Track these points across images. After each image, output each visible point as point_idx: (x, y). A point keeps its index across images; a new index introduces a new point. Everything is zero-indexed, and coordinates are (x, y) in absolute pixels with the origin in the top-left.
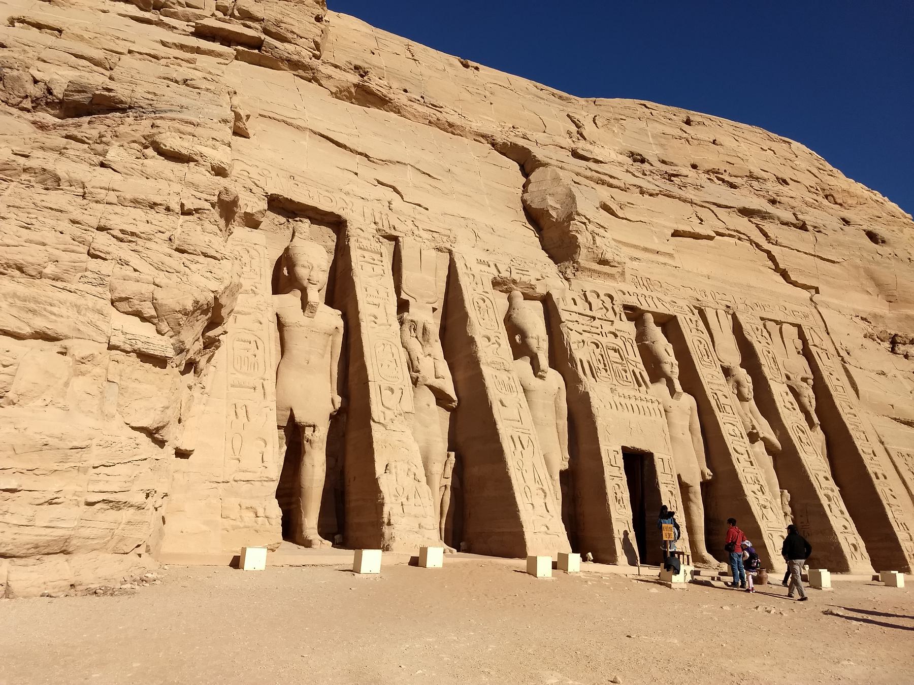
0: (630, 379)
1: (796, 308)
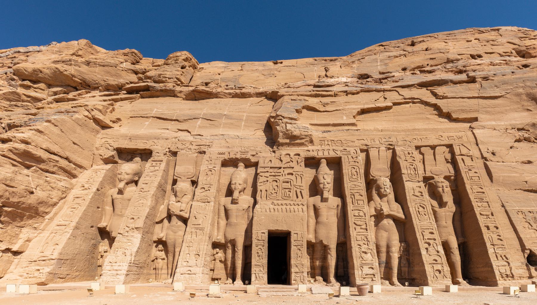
0: (291, 195)
1: (451, 134)
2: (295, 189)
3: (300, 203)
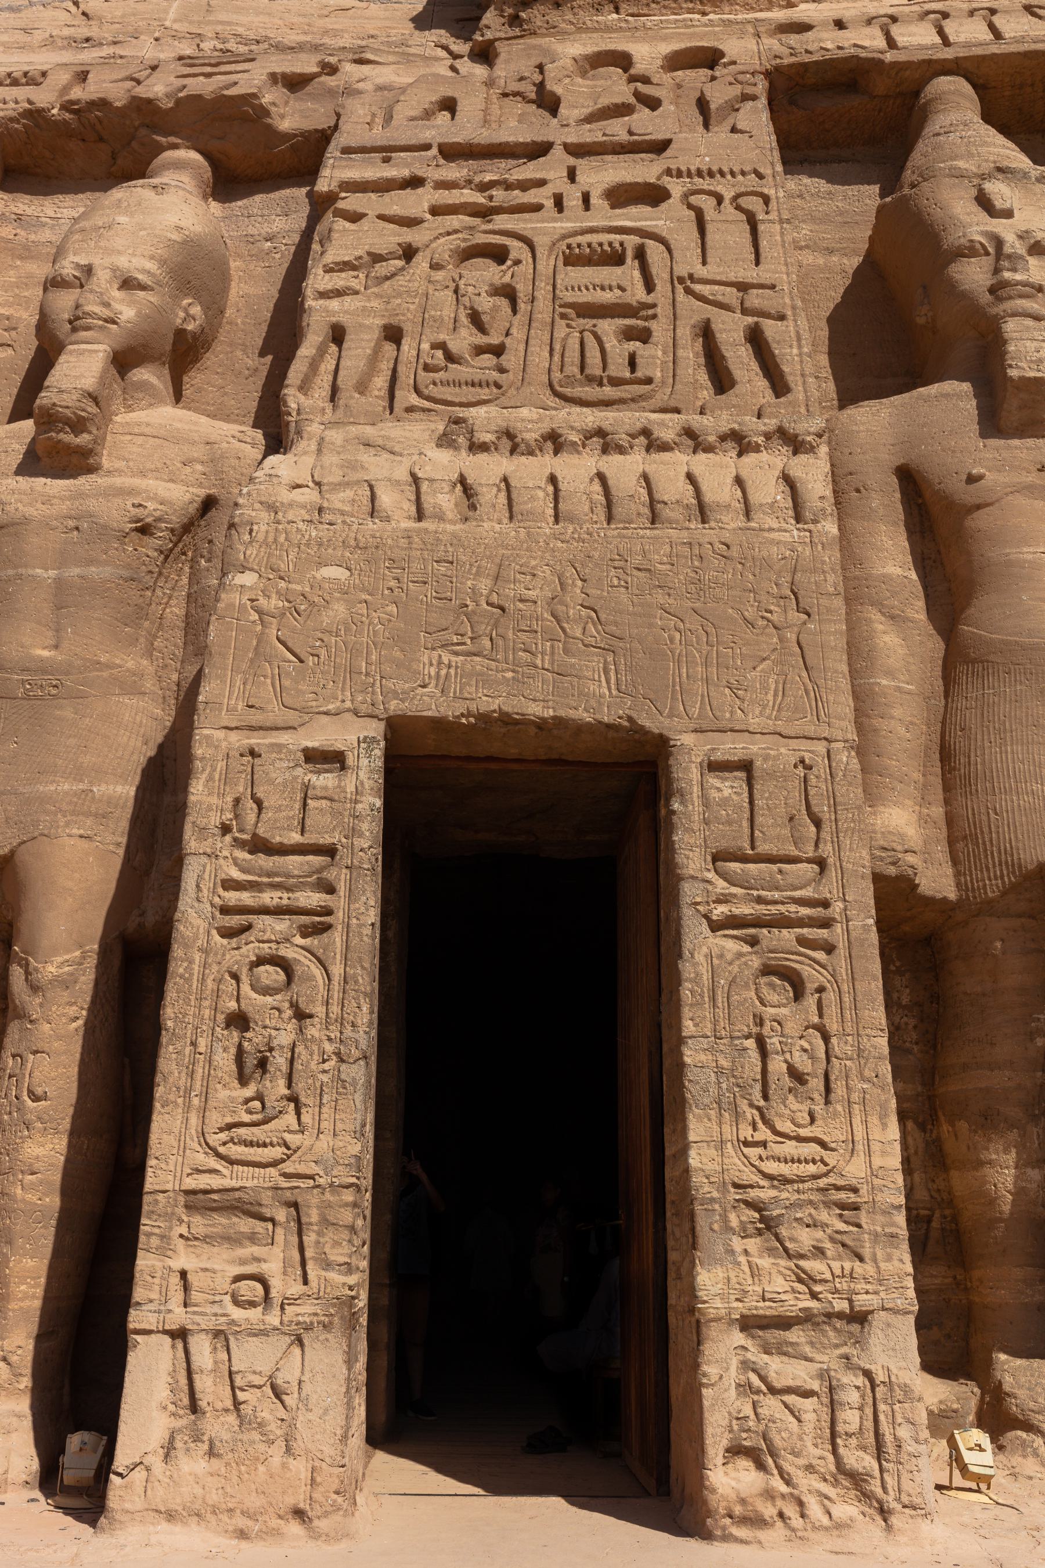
2: (692, 311)
3: (754, 427)
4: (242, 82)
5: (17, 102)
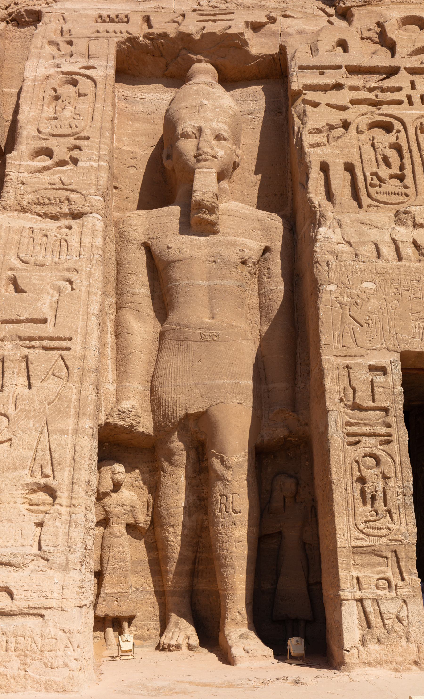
4: (233, 26)
5: (121, 33)
